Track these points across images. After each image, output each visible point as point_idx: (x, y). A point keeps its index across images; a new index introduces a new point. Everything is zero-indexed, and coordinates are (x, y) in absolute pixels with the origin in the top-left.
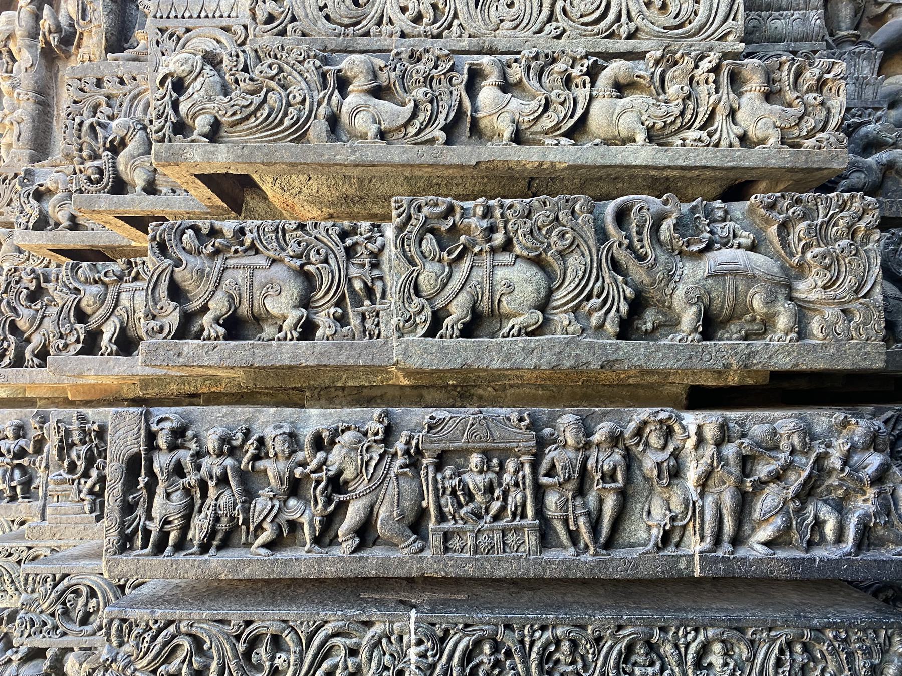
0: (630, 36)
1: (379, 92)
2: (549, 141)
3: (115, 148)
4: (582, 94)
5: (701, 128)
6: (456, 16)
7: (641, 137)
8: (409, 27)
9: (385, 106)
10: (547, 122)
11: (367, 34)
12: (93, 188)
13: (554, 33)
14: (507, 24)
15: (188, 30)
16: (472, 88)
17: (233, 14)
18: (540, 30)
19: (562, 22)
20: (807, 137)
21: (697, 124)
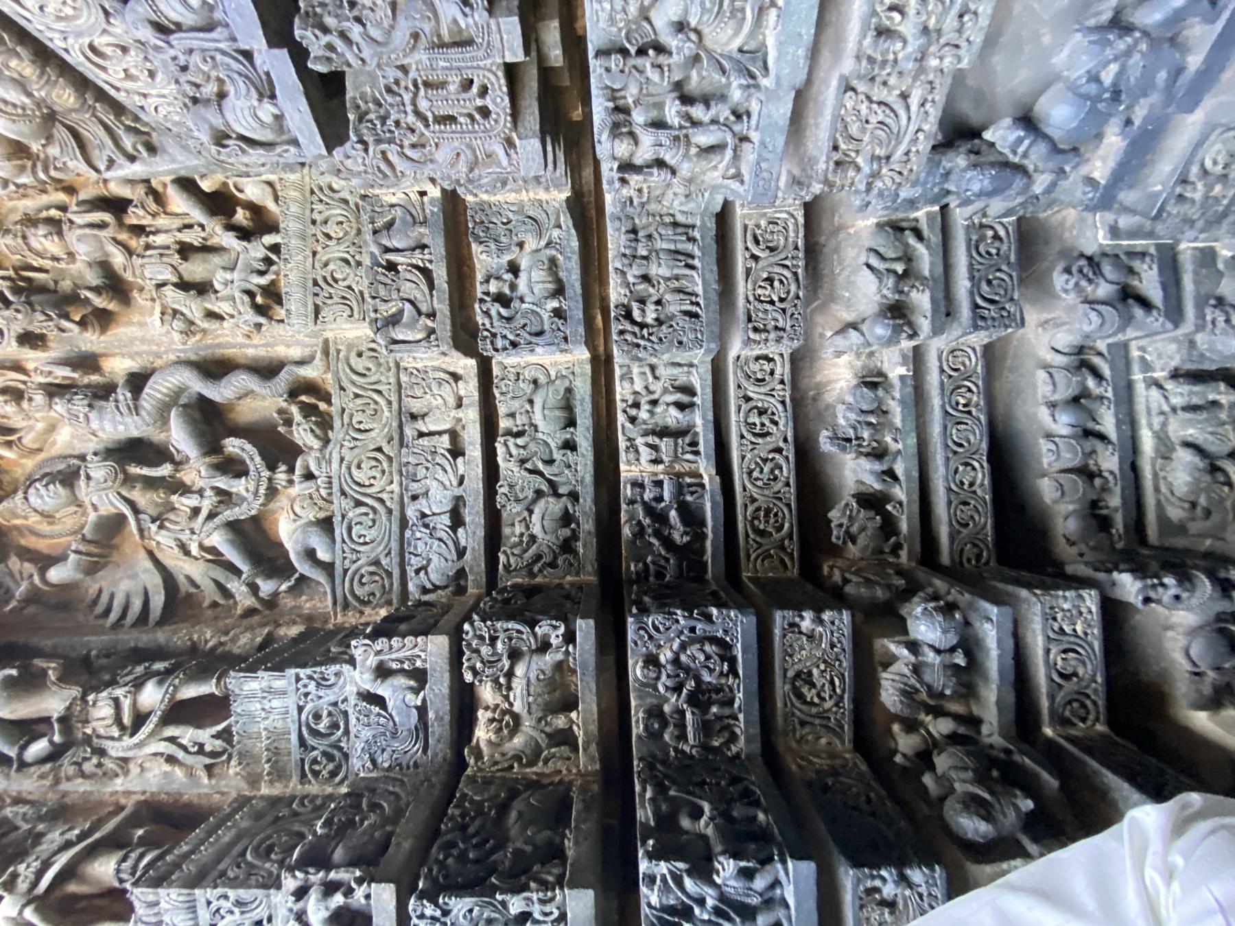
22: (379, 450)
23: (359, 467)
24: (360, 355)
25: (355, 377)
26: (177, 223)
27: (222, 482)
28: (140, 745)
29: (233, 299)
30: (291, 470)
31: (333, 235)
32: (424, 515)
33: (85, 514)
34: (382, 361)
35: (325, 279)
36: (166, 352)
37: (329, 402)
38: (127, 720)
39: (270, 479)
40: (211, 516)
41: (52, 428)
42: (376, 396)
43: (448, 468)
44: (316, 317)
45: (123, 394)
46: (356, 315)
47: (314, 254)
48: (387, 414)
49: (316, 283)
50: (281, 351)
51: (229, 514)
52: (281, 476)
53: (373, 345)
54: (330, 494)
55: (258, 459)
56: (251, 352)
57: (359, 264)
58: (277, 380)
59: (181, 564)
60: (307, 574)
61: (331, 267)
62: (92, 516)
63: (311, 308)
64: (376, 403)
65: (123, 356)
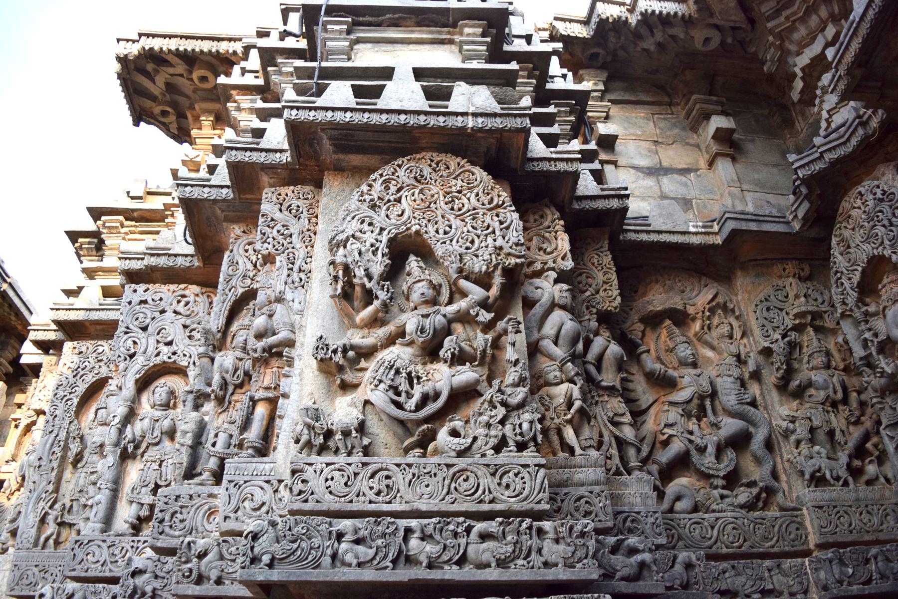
0: (491, 502)
1: (358, 542)
2: (447, 567)
3: (201, 556)
4: (463, 541)
5: (525, 559)
6: (398, 491)
7: (493, 565)
8: (374, 498)
9: (361, 549)
10: (445, 558)
11: (351, 502)
12: (185, 580)
13: (451, 501)
14: (425, 496)
15: (245, 482)
16: (406, 539)
17: (272, 473)
18: (443, 499)
19: (455, 495)
20: (578, 562)
21: (522, 556)
22: (745, 541)
23: (734, 528)
24: (797, 529)
25: (784, 526)
26: (844, 428)
27: (711, 449)
28: (605, 425)
29: (812, 458)
30: (723, 488)
31: (862, 516)
32: (724, 572)
33: (675, 369)
34: (796, 543)
35: (838, 512)
36: (768, 413)
37: (762, 509)
38: (616, 419)
39: (718, 477)
40: (691, 441)
41: (712, 348)
42: (775, 539)
43: (754, 588)
44: (816, 507)
45: (747, 398)
46: (823, 530)
47: (850, 506)
48: (767, 545)
49: (835, 507)
50: (783, 477)
51: (694, 452)
52: (720, 482)
53: (804, 537)
54: (714, 511)
55: (728, 469)
56: (778, 460)
57: (851, 532)
58: (774, 481)
59: (653, 418)
60: (666, 497)
61: (846, 516)
62: (675, 374)
63: (821, 503)
64: (772, 539)
65: (761, 389)
